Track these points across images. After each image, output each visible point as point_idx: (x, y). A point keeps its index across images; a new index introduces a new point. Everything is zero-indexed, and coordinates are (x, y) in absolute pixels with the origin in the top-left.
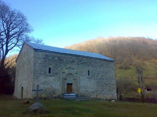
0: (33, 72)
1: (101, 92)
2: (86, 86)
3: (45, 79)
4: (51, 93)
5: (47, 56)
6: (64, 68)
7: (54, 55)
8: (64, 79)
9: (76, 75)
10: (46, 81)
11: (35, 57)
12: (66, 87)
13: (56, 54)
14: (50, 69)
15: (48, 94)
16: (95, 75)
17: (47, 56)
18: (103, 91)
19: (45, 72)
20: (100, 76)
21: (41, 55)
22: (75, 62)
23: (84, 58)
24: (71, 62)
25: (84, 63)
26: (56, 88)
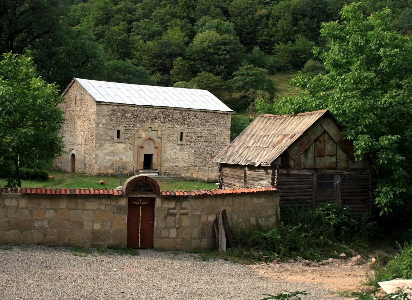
0: (94, 137)
1: (199, 169)
2: (176, 158)
3: (112, 148)
4: (120, 168)
5: (114, 111)
6: (141, 130)
7: (125, 108)
8: (139, 148)
9: (159, 140)
10: (114, 150)
11: (98, 115)
12: (142, 159)
13: (129, 108)
14: (119, 132)
15: (116, 170)
16: (193, 140)
17: (114, 111)
18: (205, 166)
19: (112, 138)
20: (203, 140)
21: (106, 110)
22: (159, 119)
23: (175, 111)
24: (152, 119)
25: (174, 119)
26: (128, 161)
